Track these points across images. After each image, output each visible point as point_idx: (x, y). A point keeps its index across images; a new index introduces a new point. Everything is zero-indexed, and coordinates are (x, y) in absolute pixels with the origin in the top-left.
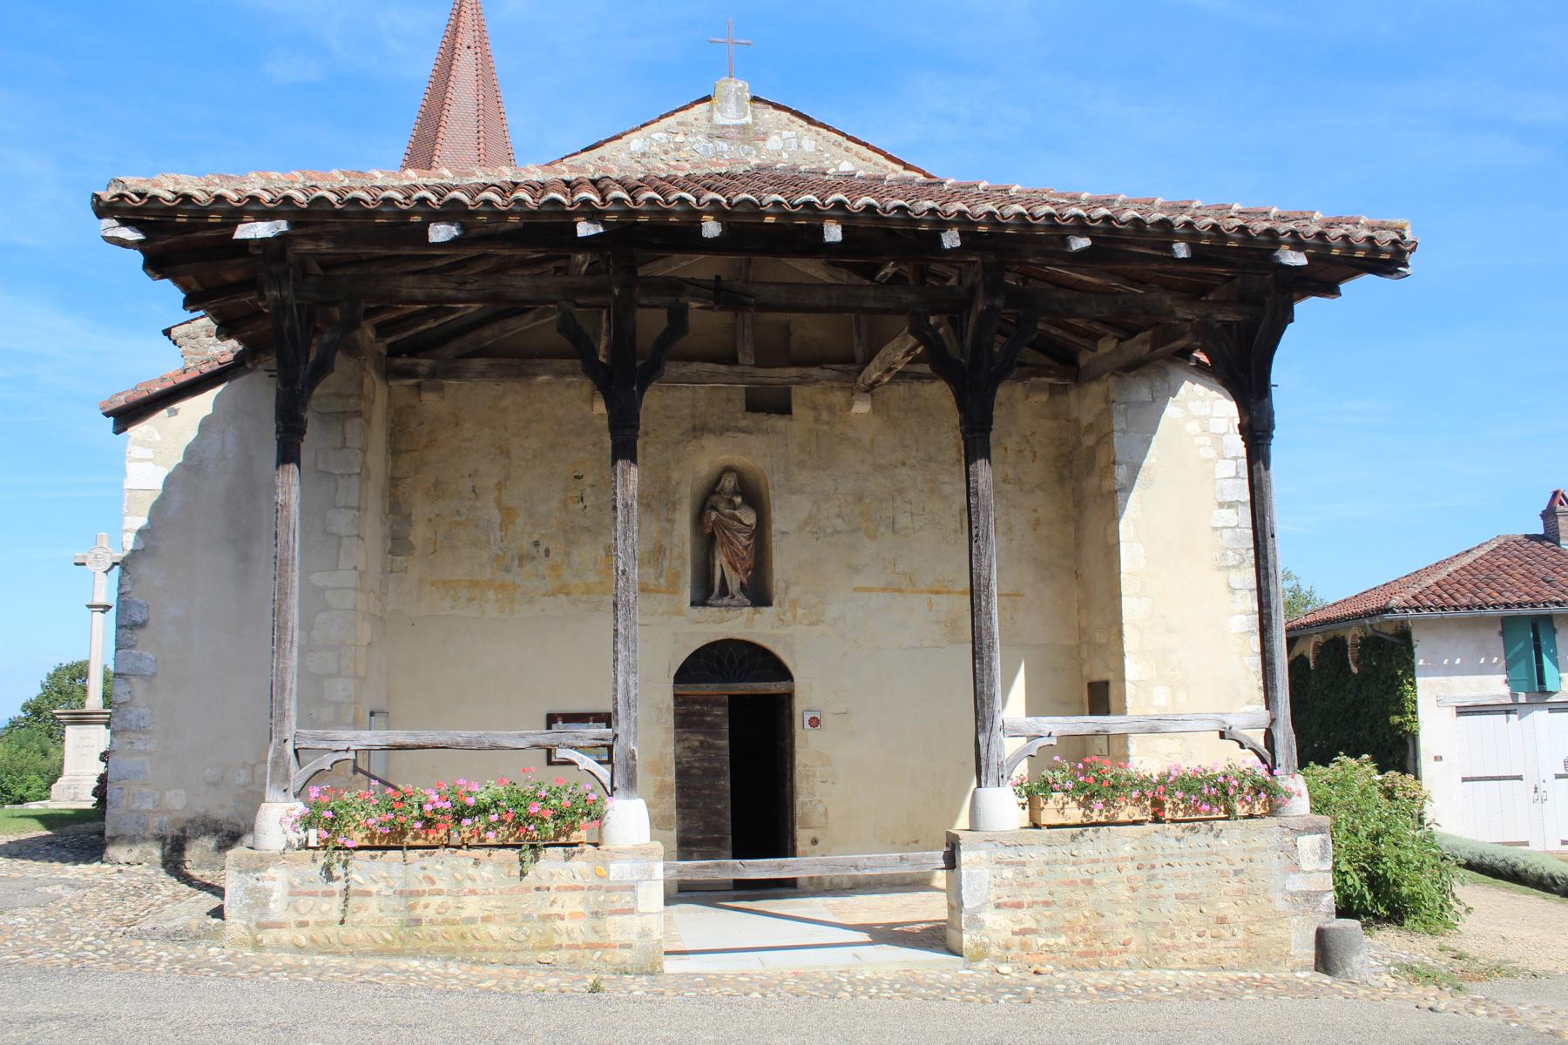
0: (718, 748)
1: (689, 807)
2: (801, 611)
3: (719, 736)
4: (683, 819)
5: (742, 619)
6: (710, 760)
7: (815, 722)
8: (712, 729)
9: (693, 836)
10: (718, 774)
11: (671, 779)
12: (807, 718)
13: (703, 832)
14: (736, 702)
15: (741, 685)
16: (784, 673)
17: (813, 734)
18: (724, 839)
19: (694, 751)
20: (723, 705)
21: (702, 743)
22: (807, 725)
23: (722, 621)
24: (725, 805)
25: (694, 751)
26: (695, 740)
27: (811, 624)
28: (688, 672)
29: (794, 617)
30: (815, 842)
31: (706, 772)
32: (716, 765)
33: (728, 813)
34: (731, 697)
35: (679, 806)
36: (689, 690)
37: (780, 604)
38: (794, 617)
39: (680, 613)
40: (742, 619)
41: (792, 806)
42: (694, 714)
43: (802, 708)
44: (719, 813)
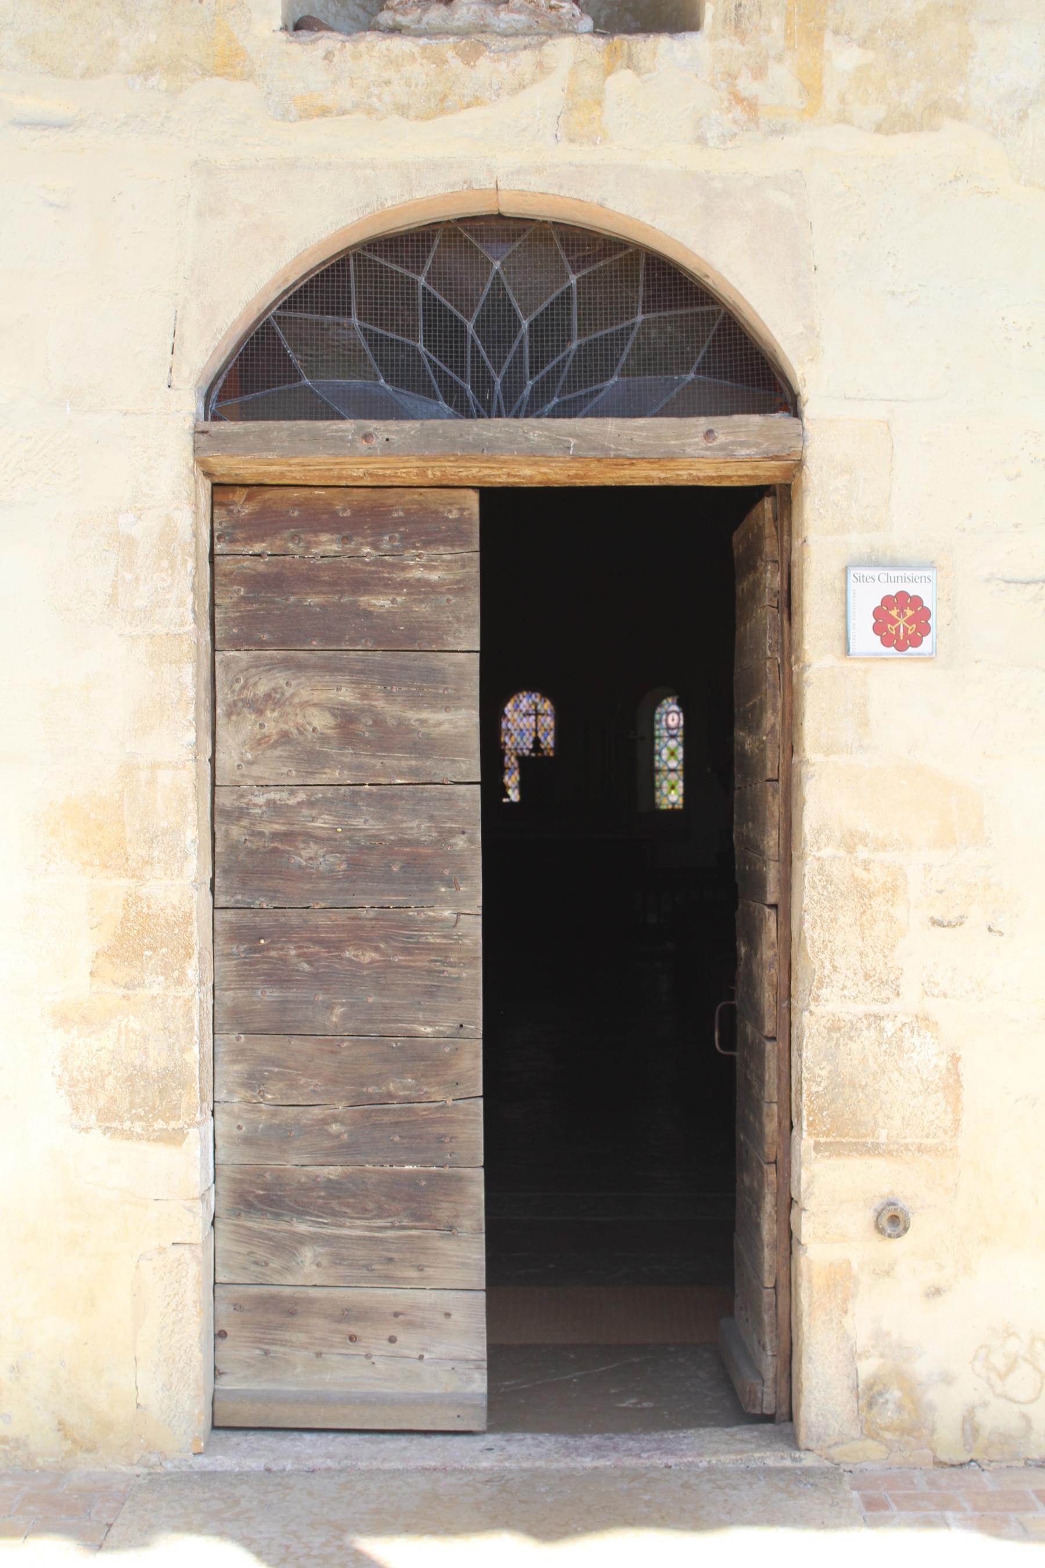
0: (426, 746)
1: (280, 1026)
2: (843, 58)
3: (428, 687)
4: (253, 1081)
5: (548, 94)
6: (384, 800)
7: (903, 623)
8: (403, 643)
9: (299, 1165)
10: (422, 870)
11: (180, 885)
12: (867, 596)
13: (345, 1150)
14: (518, 525)
15: (536, 430)
16: (751, 376)
17: (896, 681)
18: (448, 1185)
19: (311, 758)
20: (453, 536)
21: (346, 720)
22: (865, 638)
23: (441, 105)
24: (455, 1021)
25: (311, 758)
26: (315, 701)
27: (898, 122)
28: (261, 374)
29: (811, 88)
30: (892, 1221)
31: (364, 862)
32: (417, 827)
33: (471, 1062)
34: (494, 499)
35: (230, 1020)
36: (286, 451)
37: (737, 22)
38: (811, 88)
39: (229, 64)
40: (548, 94)
41: (786, 1034)
42: (310, 579)
43: (835, 565)
44: (424, 1059)
